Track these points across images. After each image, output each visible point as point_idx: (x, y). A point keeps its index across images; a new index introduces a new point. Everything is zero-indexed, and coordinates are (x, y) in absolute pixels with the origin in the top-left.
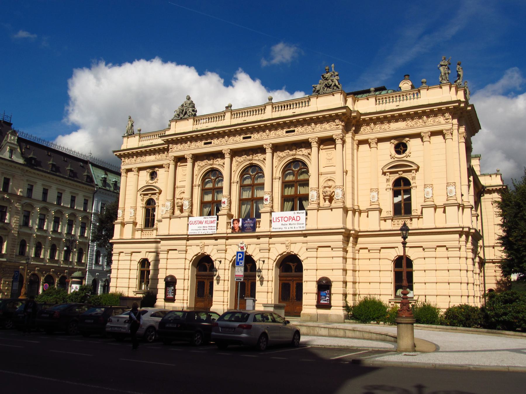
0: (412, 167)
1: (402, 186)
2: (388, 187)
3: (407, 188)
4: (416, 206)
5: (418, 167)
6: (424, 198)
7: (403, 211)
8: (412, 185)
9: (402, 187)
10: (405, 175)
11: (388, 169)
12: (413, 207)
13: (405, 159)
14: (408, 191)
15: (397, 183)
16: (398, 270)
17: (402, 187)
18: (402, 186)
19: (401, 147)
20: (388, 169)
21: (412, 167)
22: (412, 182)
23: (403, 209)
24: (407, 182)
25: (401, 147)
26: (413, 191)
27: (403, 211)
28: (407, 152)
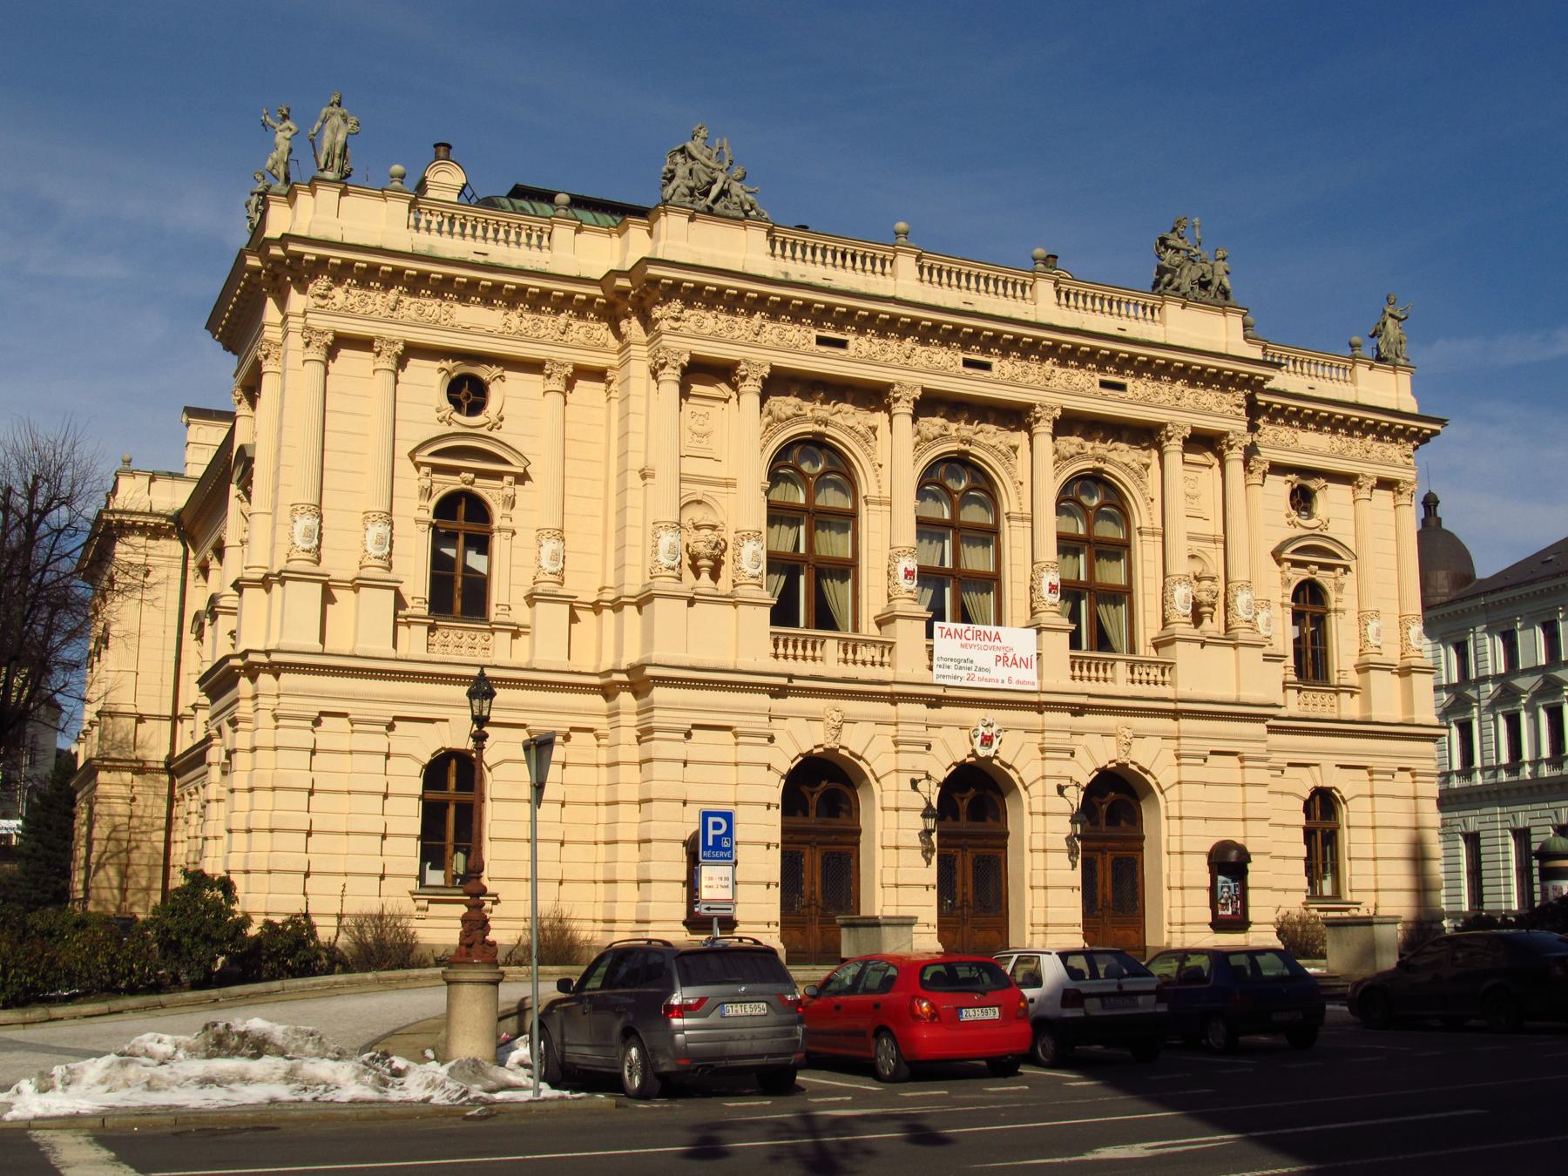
0: (507, 462)
1: (462, 520)
3: (474, 527)
4: (504, 595)
7: (458, 604)
8: (497, 522)
9: (461, 524)
10: (483, 488)
11: (434, 454)
13: (484, 431)
14: (482, 544)
16: (434, 795)
17: (461, 524)
18: (462, 520)
19: (467, 393)
20: (434, 454)
21: (507, 462)
23: (458, 595)
24: (478, 509)
25: (467, 393)
27: (458, 604)
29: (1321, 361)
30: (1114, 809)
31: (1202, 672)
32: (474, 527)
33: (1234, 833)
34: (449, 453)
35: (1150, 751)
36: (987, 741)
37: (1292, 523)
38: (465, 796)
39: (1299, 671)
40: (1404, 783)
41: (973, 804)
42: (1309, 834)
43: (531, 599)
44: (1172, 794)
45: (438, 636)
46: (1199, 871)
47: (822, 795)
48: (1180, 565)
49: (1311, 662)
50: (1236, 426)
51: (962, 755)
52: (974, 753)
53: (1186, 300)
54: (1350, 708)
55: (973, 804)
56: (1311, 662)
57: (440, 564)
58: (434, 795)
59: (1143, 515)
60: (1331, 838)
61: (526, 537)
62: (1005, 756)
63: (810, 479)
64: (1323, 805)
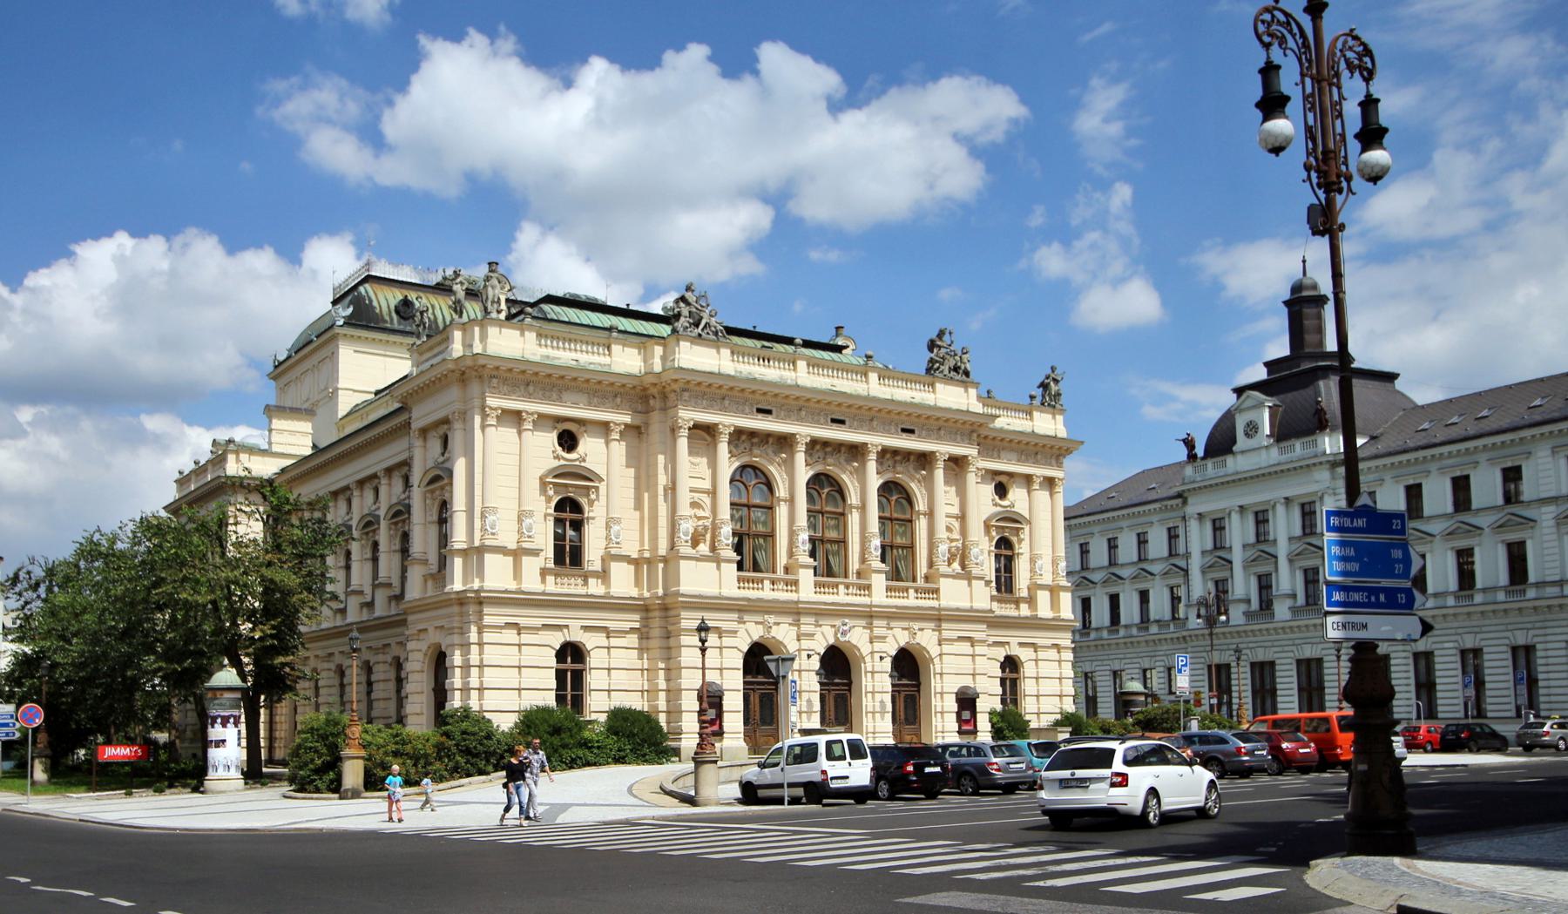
1: (570, 513)
3: (575, 516)
4: (593, 553)
6: (604, 543)
15: (560, 507)
18: (570, 513)
22: (586, 508)
23: (568, 555)
24: (576, 507)
25: (568, 441)
30: (908, 666)
31: (953, 594)
32: (575, 516)
33: (967, 681)
35: (926, 639)
38: (578, 666)
39: (998, 589)
40: (1053, 654)
41: (837, 665)
42: (1003, 681)
44: (937, 661)
46: (951, 705)
47: (760, 662)
48: (942, 533)
49: (1004, 582)
51: (832, 641)
53: (949, 380)
54: (1025, 610)
55: (837, 665)
56: (1004, 582)
57: (559, 538)
58: (562, 666)
59: (921, 505)
62: (854, 642)
64: (1011, 664)
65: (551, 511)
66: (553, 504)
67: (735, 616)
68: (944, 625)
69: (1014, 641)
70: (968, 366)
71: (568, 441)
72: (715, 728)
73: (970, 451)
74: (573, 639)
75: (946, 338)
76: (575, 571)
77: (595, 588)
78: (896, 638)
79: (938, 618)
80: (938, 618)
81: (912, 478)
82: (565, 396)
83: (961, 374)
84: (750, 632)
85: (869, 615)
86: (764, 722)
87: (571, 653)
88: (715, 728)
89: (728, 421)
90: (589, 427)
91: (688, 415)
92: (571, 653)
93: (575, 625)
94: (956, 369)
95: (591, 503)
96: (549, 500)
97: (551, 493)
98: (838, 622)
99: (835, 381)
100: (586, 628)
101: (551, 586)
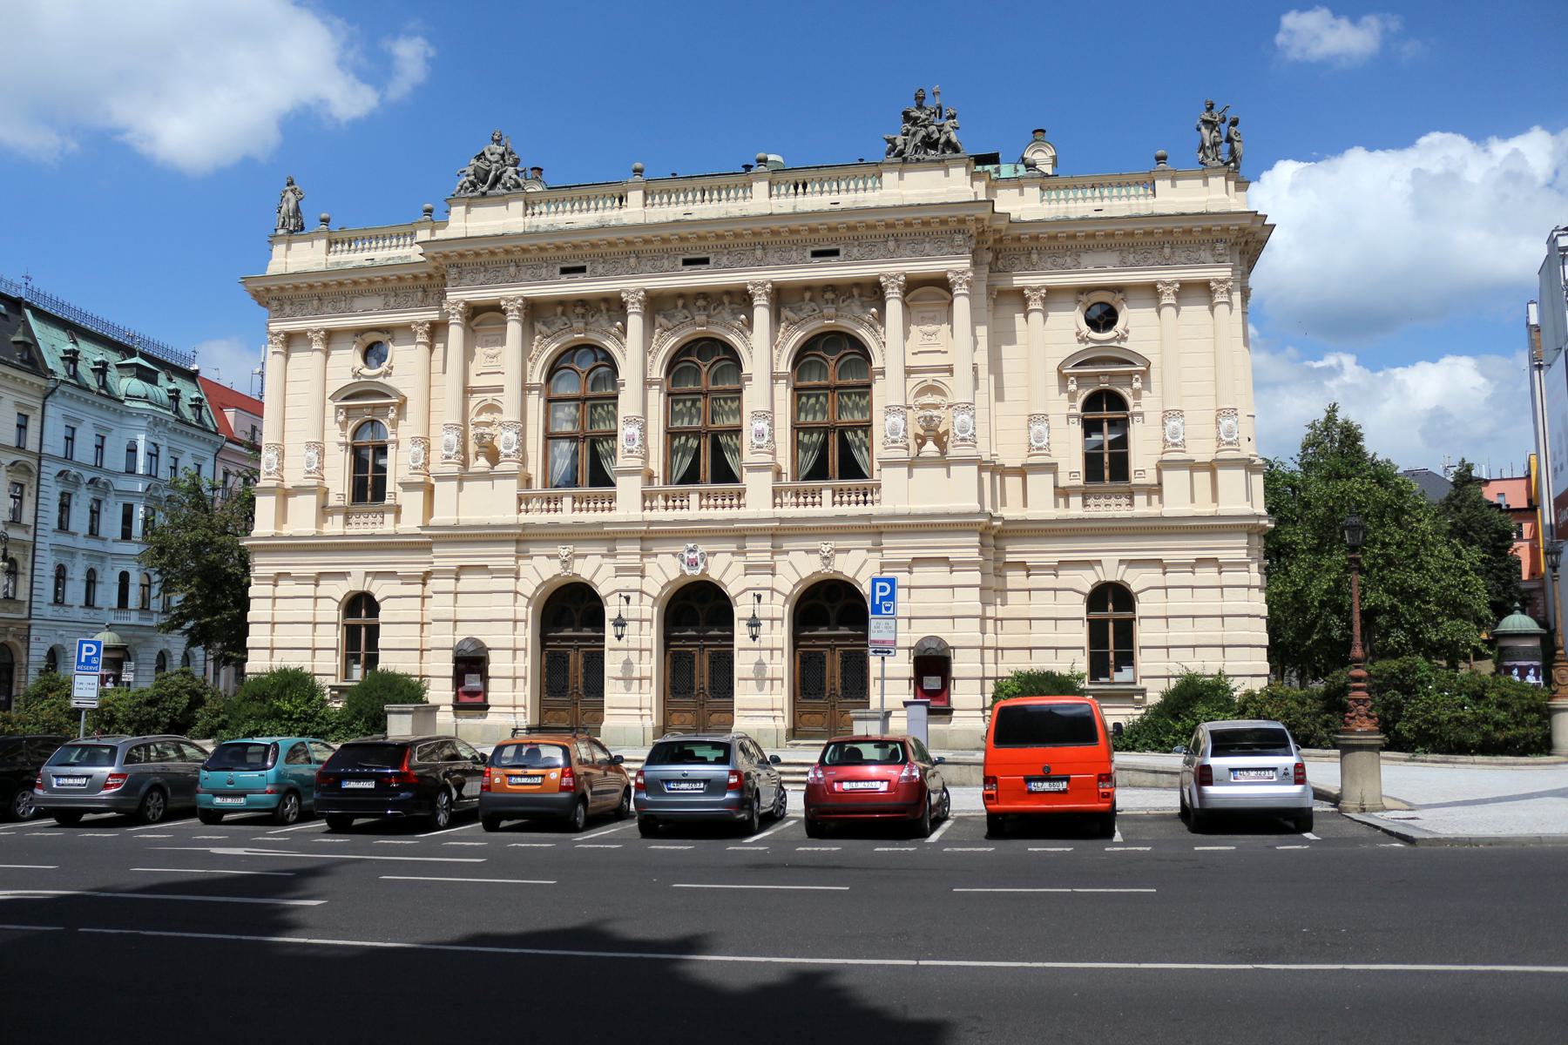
2: (343, 440)
5: (405, 400)
12: (389, 487)
13: (381, 379)
19: (373, 352)
21: (388, 396)
22: (389, 429)
25: (373, 352)
26: (391, 451)
28: (385, 366)
29: (1114, 182)
34: (353, 394)
36: (693, 564)
37: (1082, 340)
41: (697, 613)
43: (407, 486)
45: (353, 519)
50: (957, 266)
52: (683, 574)
55: (697, 613)
60: (1126, 632)
61: (406, 444)
63: (582, 377)
65: (1078, 410)
66: (349, 432)
67: (512, 549)
68: (886, 542)
69: (358, 571)
70: (954, 137)
71: (1103, 318)
72: (479, 699)
73: (957, 266)
74: (1111, 577)
75: (930, 104)
76: (378, 506)
77: (387, 525)
78: (800, 566)
79: (876, 531)
80: (876, 531)
81: (860, 321)
82: (359, 303)
83: (934, 149)
84: (542, 570)
85: (739, 535)
86: (588, 692)
87: (361, 606)
88: (479, 699)
89: (511, 294)
90: (398, 335)
91: (458, 297)
92: (361, 606)
93: (358, 571)
94: (929, 143)
95: (394, 424)
96: (343, 426)
97: (341, 418)
98: (680, 549)
99: (690, 208)
100: (377, 575)
101: (335, 526)
